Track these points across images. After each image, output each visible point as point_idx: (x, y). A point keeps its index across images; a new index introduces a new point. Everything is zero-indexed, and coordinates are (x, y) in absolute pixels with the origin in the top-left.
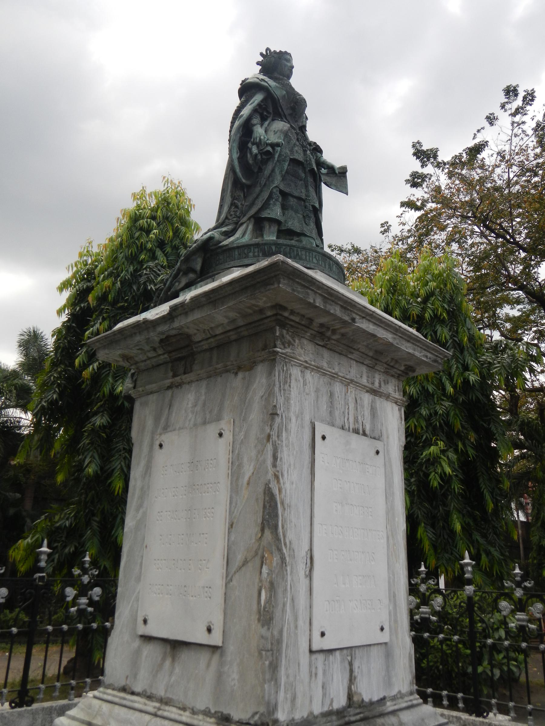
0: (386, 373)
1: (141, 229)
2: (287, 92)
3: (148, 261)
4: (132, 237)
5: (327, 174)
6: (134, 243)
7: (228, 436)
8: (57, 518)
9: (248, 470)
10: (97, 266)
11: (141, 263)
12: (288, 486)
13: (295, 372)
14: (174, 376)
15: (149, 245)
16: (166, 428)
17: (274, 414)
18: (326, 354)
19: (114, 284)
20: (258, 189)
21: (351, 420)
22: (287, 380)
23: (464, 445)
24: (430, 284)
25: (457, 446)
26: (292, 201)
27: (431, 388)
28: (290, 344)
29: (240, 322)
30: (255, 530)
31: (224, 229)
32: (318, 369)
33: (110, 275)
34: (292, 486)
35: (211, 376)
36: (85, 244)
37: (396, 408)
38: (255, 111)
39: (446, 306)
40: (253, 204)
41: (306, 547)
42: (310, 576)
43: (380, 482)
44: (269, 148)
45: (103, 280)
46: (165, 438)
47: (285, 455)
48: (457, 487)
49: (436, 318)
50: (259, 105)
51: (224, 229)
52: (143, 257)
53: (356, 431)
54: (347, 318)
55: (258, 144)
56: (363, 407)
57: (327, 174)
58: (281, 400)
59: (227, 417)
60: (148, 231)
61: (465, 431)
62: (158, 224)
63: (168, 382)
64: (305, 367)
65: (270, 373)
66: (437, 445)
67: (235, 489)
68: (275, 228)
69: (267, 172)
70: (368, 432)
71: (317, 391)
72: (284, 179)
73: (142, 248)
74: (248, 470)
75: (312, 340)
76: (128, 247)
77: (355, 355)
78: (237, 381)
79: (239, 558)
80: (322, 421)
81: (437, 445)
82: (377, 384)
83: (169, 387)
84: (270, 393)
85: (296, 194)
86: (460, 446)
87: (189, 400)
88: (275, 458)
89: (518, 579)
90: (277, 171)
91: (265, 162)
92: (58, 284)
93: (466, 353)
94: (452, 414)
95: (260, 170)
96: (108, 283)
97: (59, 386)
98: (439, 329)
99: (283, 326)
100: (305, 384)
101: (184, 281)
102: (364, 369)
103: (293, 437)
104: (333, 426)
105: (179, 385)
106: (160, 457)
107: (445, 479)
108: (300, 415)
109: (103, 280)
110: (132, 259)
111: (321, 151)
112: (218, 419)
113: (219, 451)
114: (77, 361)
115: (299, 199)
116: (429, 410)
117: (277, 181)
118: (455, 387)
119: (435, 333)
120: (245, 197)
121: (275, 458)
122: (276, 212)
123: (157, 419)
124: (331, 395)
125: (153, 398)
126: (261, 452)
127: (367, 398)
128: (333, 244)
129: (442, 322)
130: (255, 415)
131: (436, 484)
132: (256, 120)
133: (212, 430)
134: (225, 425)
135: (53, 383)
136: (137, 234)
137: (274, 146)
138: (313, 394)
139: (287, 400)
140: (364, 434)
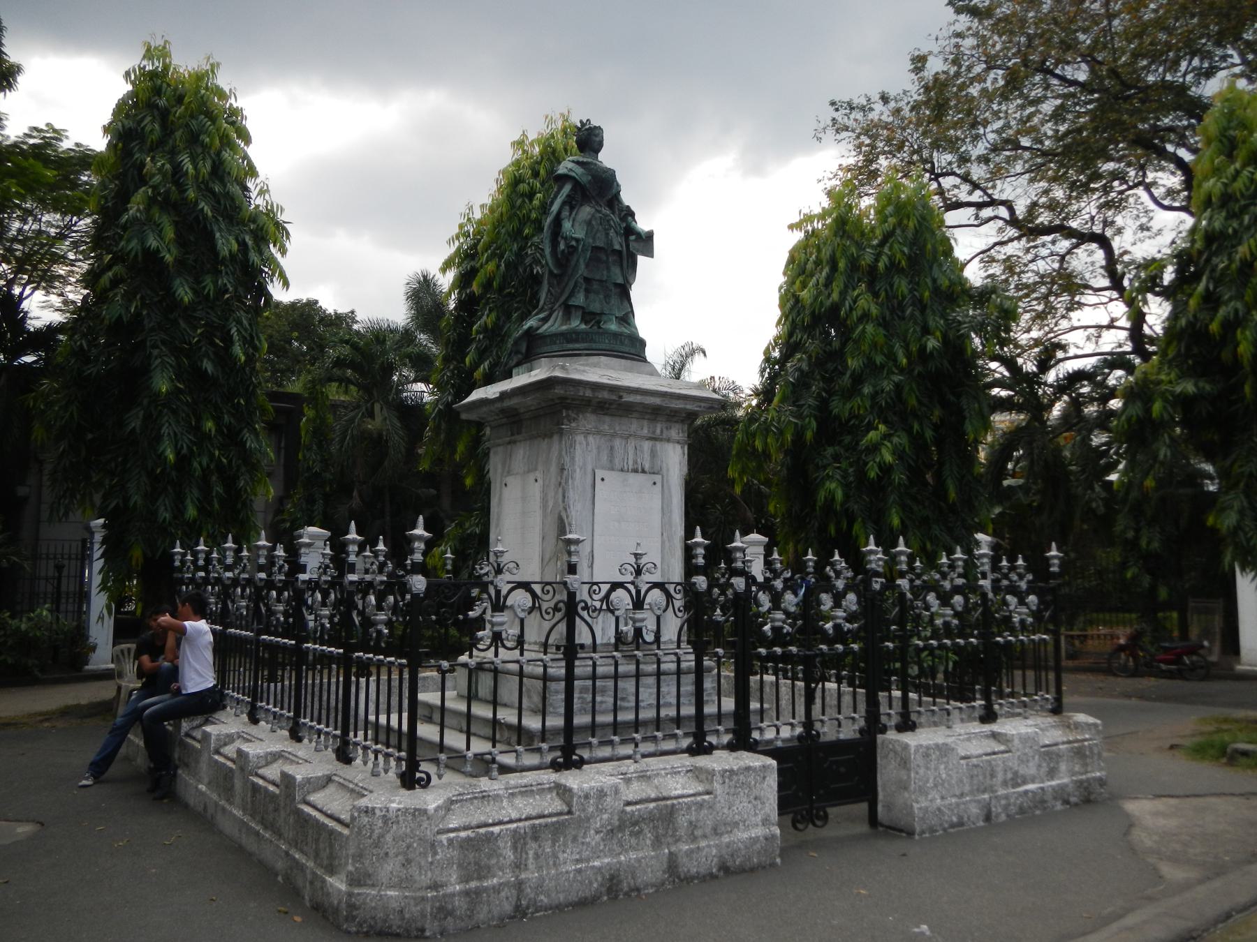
0: (668, 421)
1: (523, 195)
2: (593, 177)
3: (533, 236)
4: (513, 206)
5: (636, 240)
6: (515, 214)
7: (540, 481)
8: (467, 525)
9: (551, 504)
10: (479, 241)
11: (527, 238)
12: (573, 513)
13: (580, 438)
14: (512, 435)
15: (534, 215)
16: (509, 473)
17: (563, 469)
18: (607, 419)
19: (498, 266)
20: (566, 279)
21: (631, 463)
22: (573, 445)
23: (921, 424)
24: (890, 219)
25: (912, 427)
26: (595, 286)
27: (879, 359)
28: (574, 419)
29: (543, 405)
30: (554, 541)
31: (541, 316)
32: (599, 433)
33: (493, 255)
34: (577, 511)
35: (532, 438)
36: (464, 209)
37: (678, 447)
38: (564, 203)
39: (906, 250)
40: (561, 294)
41: (589, 550)
42: (591, 566)
43: (657, 503)
44: (574, 243)
45: (487, 262)
46: (509, 480)
47: (571, 494)
48: (899, 477)
49: (893, 267)
50: (568, 196)
51: (541, 316)
52: (527, 231)
53: (635, 471)
54: (614, 397)
55: (565, 239)
56: (642, 452)
57: (636, 240)
58: (567, 459)
59: (540, 468)
60: (531, 195)
61: (924, 409)
62: (542, 184)
63: (508, 439)
64: (587, 434)
65: (560, 441)
66: (877, 429)
67: (545, 516)
68: (580, 313)
69: (573, 263)
70: (647, 468)
71: (598, 448)
72: (587, 266)
73: (525, 220)
74: (551, 504)
75: (594, 412)
76: (510, 219)
77: (635, 415)
78: (544, 444)
79: (547, 557)
80: (603, 468)
81: (877, 429)
82: (658, 431)
83: (509, 443)
84: (560, 456)
85: (598, 277)
86: (916, 426)
87: (521, 454)
88: (564, 497)
89: (918, 571)
90: (581, 261)
91: (571, 254)
92: (440, 265)
93: (928, 311)
94: (907, 388)
95: (568, 260)
96: (491, 267)
97: (453, 386)
98: (896, 280)
99: (567, 408)
100: (587, 444)
101: (515, 361)
102: (645, 422)
103: (577, 482)
104: (613, 469)
105: (515, 442)
106: (506, 491)
107: (886, 469)
108: (583, 468)
109: (487, 262)
110: (517, 234)
111: (632, 214)
112: (536, 469)
113: (535, 490)
114: (467, 360)
115: (601, 281)
116: (874, 387)
117: (582, 270)
118: (908, 355)
119: (892, 286)
120: (558, 284)
121: (564, 497)
122: (580, 299)
123: (504, 464)
124: (612, 448)
125: (500, 449)
126: (556, 493)
127: (647, 445)
128: (837, 100)
129: (901, 271)
130: (554, 469)
131: (872, 475)
132: (565, 213)
133: (532, 477)
134: (538, 474)
135: (447, 383)
136: (519, 201)
137: (577, 240)
138: (595, 451)
139: (573, 458)
140: (643, 471)
